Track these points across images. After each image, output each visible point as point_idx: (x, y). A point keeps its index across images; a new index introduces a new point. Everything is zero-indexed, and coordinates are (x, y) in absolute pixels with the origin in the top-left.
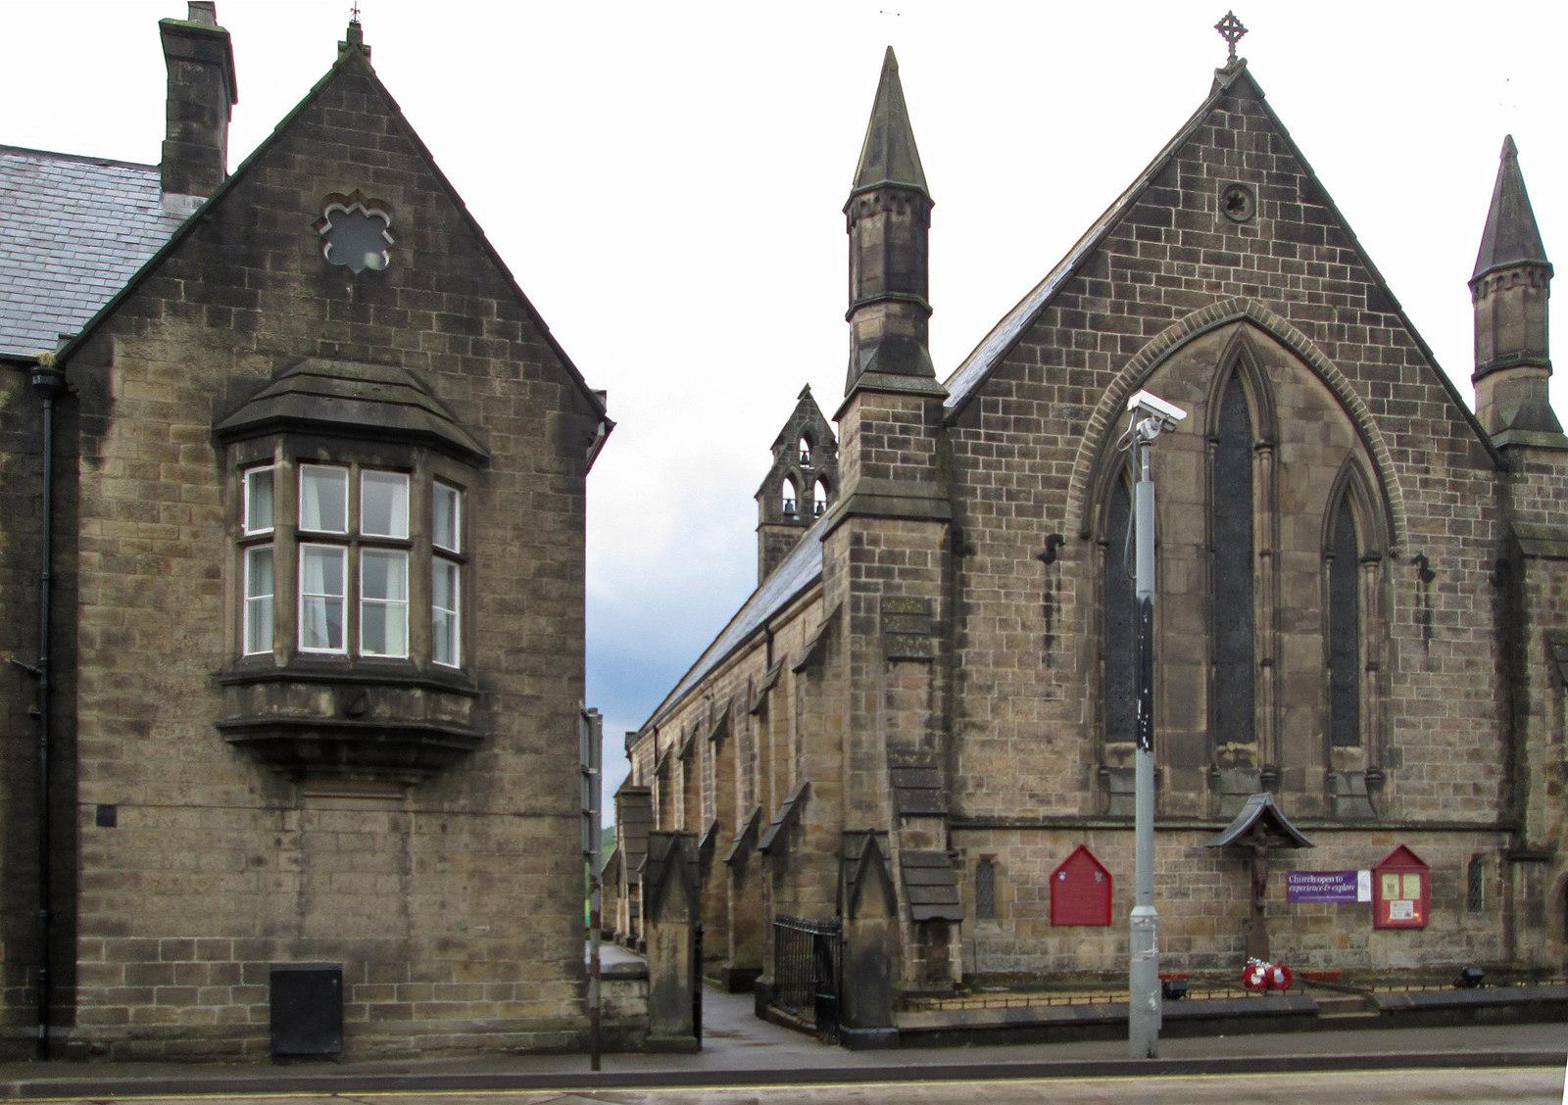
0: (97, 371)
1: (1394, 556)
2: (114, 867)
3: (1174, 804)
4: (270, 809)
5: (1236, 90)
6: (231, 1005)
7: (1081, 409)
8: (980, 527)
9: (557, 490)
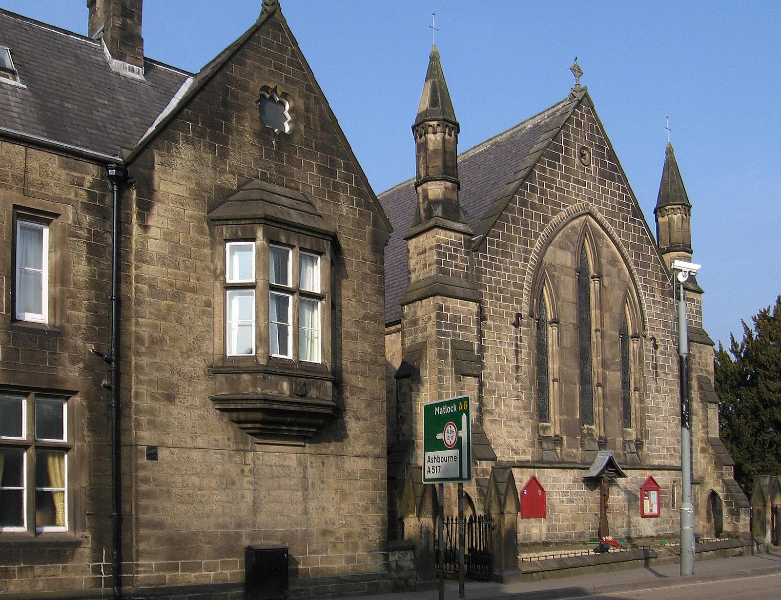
0: (146, 172)
1: (645, 337)
2: (157, 486)
3: (568, 455)
4: (238, 451)
5: (582, 101)
6: (220, 571)
7: (527, 249)
8: (489, 307)
9: (372, 272)
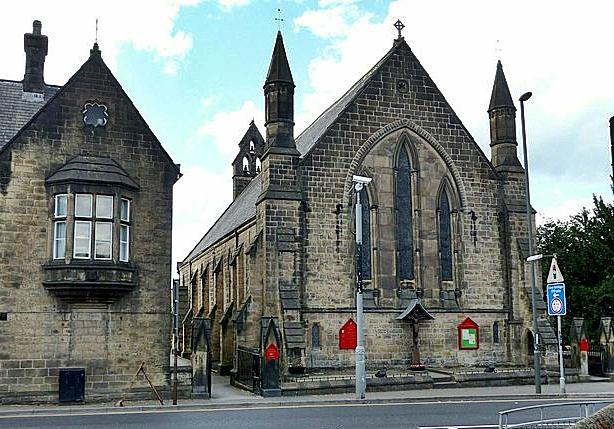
8: (312, 202)
